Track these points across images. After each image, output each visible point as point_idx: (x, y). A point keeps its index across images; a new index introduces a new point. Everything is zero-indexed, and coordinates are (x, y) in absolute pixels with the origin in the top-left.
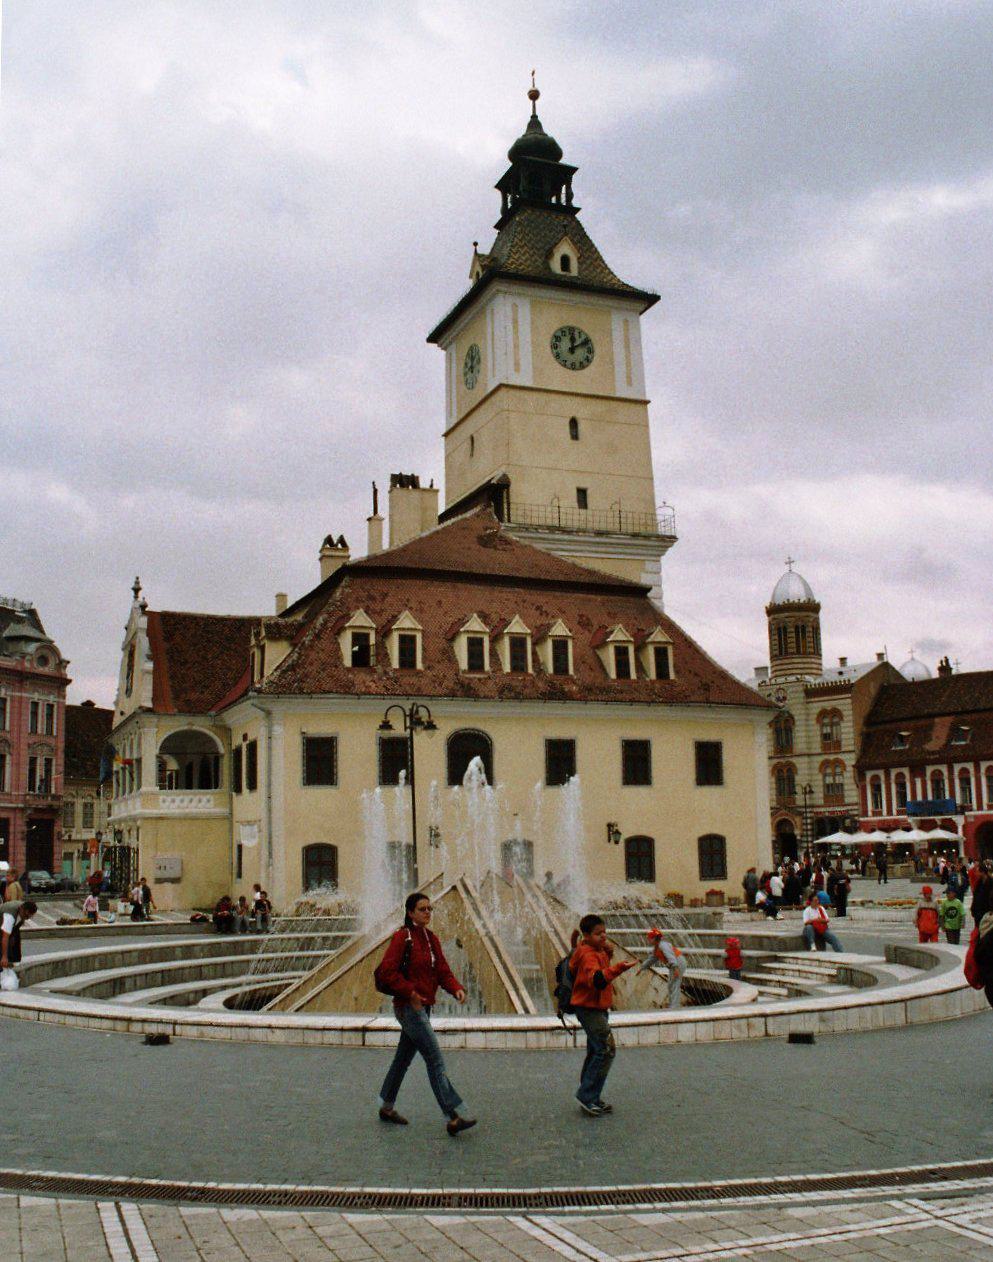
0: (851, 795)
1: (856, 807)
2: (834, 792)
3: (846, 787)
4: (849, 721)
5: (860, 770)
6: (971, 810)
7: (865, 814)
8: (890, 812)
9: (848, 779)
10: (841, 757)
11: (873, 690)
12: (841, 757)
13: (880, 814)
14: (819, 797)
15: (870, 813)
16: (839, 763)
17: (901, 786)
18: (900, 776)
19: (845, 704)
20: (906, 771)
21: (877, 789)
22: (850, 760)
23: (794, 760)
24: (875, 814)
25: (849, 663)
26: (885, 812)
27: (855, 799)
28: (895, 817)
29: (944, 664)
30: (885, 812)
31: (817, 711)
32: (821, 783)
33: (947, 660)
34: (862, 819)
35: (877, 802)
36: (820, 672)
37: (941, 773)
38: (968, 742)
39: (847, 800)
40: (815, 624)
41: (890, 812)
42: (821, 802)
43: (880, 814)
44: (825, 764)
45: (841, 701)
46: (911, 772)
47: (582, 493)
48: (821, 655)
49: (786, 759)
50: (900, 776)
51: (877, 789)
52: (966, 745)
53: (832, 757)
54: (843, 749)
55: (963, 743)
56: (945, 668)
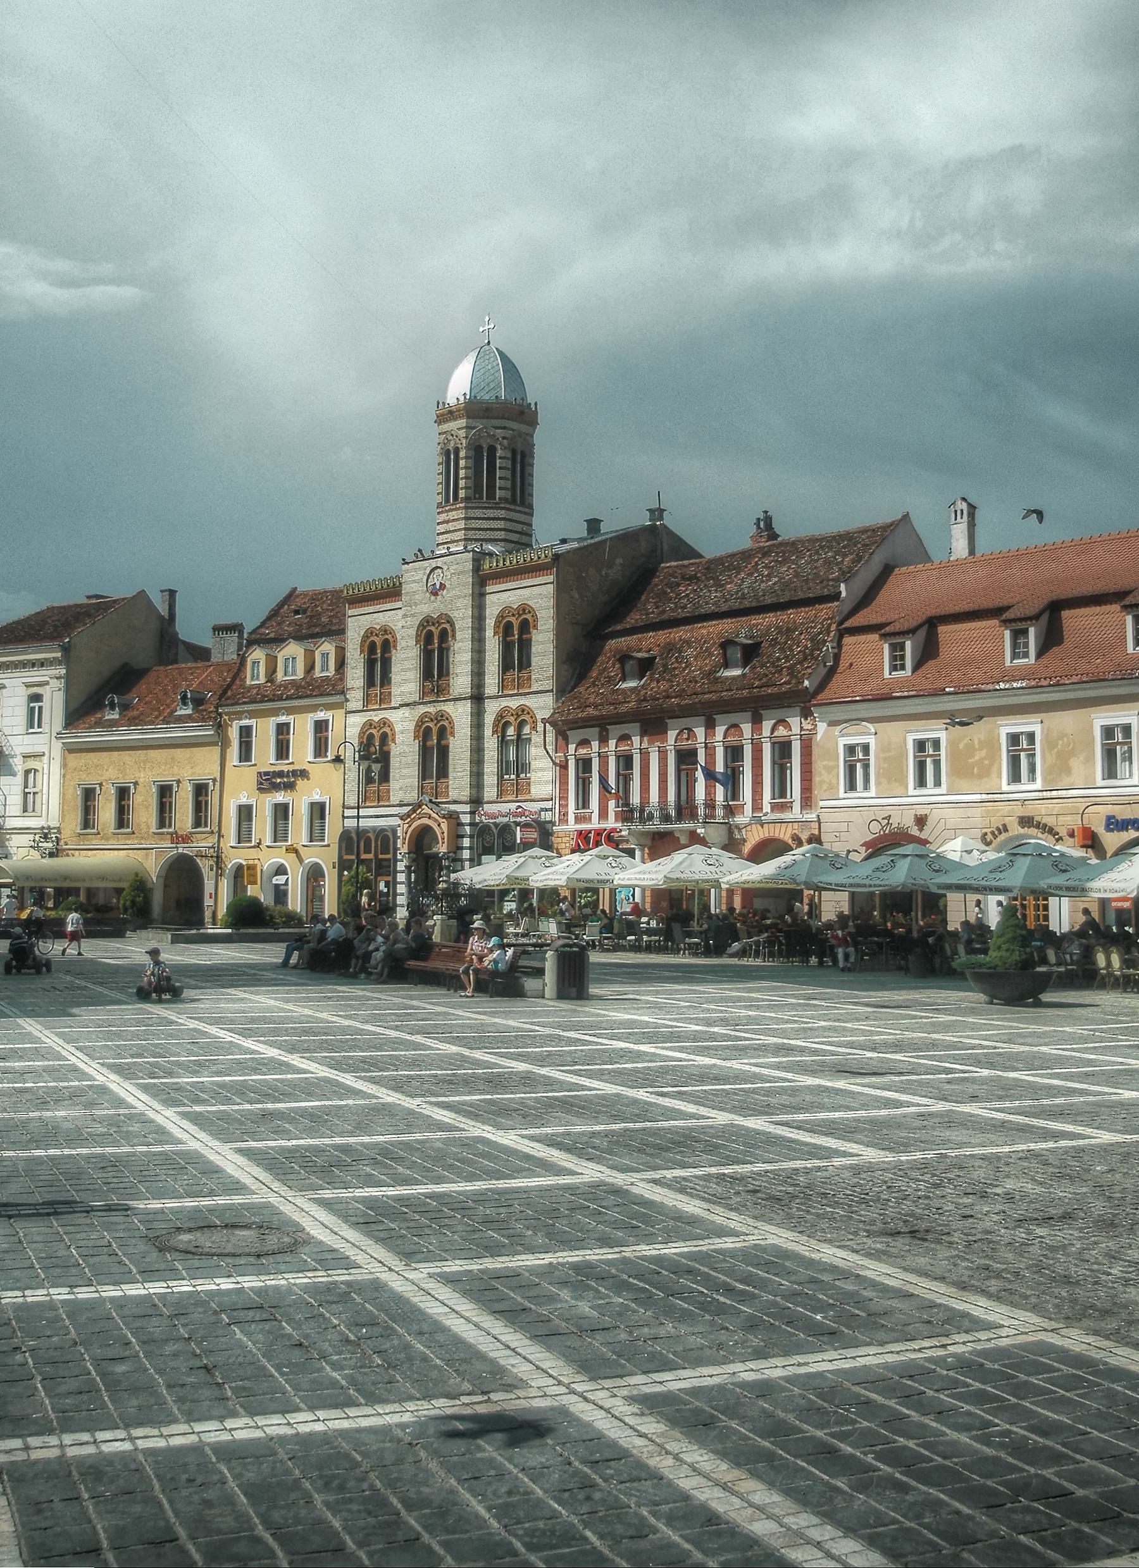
1: (549, 805)
8: (603, 814)
10: (530, 702)
12: (530, 702)
13: (588, 819)
15: (571, 817)
16: (523, 716)
23: (449, 708)
24: (579, 819)
25: (604, 528)
26: (595, 816)
28: (611, 823)
29: (762, 524)
33: (768, 520)
36: (524, 539)
39: (536, 791)
40: (519, 447)
43: (588, 819)
45: (536, 590)
48: (531, 507)
52: (744, 675)
53: (514, 703)
54: (534, 688)
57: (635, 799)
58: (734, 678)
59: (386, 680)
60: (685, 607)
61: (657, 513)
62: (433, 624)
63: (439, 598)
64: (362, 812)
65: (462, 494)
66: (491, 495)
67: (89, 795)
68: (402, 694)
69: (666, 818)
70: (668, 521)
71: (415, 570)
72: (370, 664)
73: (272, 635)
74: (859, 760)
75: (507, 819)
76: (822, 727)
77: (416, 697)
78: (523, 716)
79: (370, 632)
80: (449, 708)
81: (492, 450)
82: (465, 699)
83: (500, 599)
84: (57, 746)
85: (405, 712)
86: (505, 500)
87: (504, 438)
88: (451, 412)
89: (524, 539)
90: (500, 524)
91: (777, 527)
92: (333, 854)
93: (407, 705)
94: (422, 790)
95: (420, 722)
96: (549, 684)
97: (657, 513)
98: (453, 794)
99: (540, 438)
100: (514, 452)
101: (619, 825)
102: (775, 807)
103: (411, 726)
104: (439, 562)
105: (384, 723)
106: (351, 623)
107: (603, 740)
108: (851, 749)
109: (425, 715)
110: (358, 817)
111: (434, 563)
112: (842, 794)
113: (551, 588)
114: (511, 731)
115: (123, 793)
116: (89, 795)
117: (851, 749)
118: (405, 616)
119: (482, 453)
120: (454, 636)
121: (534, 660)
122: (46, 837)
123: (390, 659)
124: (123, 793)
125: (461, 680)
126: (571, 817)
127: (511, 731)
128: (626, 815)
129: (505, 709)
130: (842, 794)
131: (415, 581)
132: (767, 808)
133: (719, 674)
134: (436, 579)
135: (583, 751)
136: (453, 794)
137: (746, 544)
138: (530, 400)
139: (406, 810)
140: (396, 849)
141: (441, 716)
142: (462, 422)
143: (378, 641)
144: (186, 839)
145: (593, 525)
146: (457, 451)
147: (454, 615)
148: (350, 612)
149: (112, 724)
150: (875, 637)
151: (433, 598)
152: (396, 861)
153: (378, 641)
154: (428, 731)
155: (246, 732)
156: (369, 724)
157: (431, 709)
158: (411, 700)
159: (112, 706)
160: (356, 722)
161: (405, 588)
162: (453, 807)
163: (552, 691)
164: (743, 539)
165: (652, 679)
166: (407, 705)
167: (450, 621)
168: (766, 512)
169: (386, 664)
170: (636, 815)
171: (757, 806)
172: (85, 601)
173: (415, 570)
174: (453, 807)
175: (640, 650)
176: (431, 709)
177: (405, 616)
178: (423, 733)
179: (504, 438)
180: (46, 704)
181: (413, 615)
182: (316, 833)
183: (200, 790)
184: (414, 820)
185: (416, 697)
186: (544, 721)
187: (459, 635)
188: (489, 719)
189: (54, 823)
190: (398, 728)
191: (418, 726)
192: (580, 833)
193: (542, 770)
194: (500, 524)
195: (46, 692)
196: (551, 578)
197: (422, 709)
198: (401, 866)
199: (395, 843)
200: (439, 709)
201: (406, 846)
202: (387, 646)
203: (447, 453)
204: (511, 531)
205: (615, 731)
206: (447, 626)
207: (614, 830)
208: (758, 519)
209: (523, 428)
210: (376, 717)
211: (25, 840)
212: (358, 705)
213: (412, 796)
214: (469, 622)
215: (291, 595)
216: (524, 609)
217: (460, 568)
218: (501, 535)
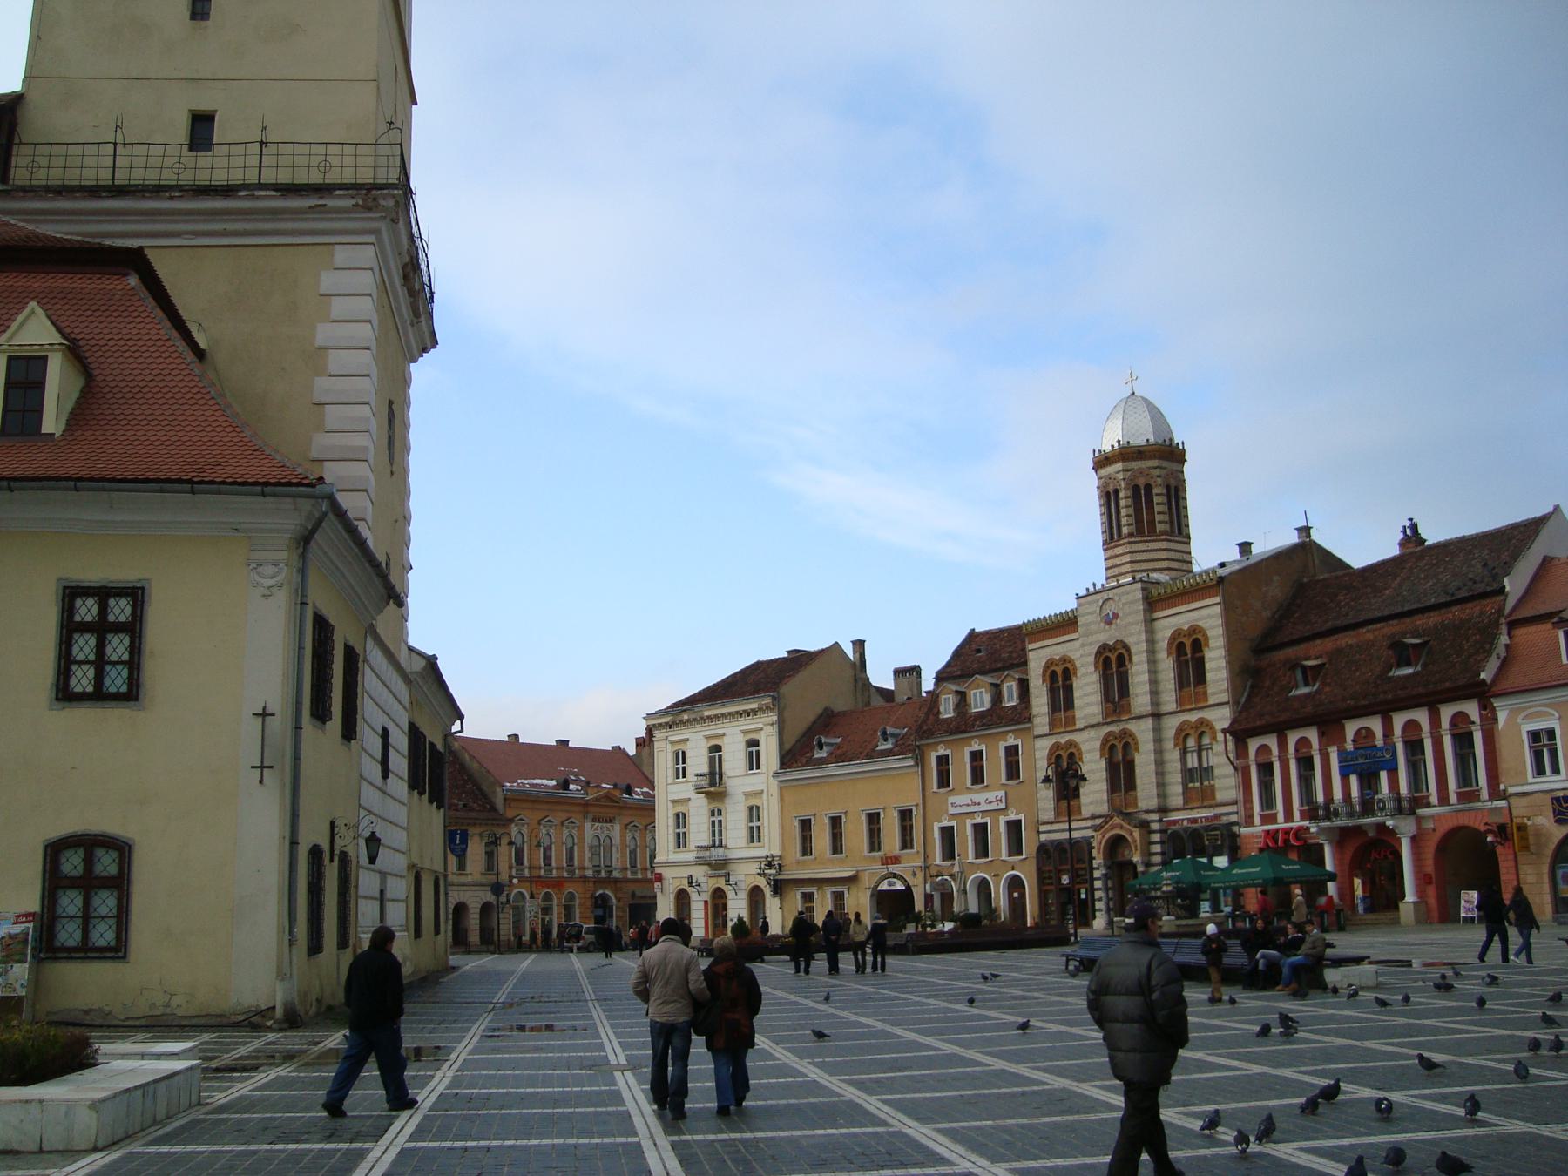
0: (1225, 784)
2: (1198, 780)
3: (1217, 772)
4: (1219, 648)
5: (1240, 734)
6: (1428, 805)
7: (1249, 821)
8: (1289, 816)
9: (1219, 757)
10: (1208, 715)
11: (1276, 590)
12: (1208, 715)
14: (1176, 796)
15: (1257, 820)
16: (1202, 728)
17: (1306, 763)
18: (1303, 743)
19: (1210, 617)
20: (1312, 735)
21: (1266, 769)
22: (1221, 718)
23: (1132, 726)
24: (1266, 819)
25: (1255, 550)
26: (1281, 817)
27: (1231, 794)
28: (1297, 822)
30: (1281, 817)
31: (1168, 633)
32: (1178, 766)
33: (1414, 527)
34: (1244, 831)
35: (1268, 801)
36: (1185, 567)
37: (1369, 733)
38: (1419, 668)
39: (1220, 796)
40: (1173, 483)
41: (1289, 816)
43: (1271, 819)
44: (1182, 734)
46: (1322, 734)
47: (201, 127)
48: (1188, 537)
49: (1122, 726)
50: (1303, 743)
51: (1266, 769)
52: (1415, 674)
53: (1193, 717)
54: (1211, 701)
55: (1408, 671)
56: (1412, 536)
57: (1320, 798)
58: (1407, 677)
59: (1069, 704)
60: (1347, 614)
61: (1305, 530)
62: (1110, 651)
63: (1113, 626)
64: (1074, 825)
65: (1125, 530)
66: (1152, 531)
67: (806, 825)
68: (1085, 717)
69: (1351, 815)
70: (1316, 536)
71: (1089, 603)
72: (1053, 692)
73: (959, 673)
74: (1545, 746)
76: (1502, 716)
77: (1099, 719)
78: (1202, 728)
79: (1050, 663)
80: (1132, 726)
81: (1148, 488)
82: (1146, 716)
83: (1172, 621)
84: (774, 784)
85: (1092, 733)
86: (1163, 533)
87: (1159, 476)
88: (1107, 458)
89: (1185, 567)
90: (1164, 555)
91: (1424, 532)
92: (1032, 867)
93: (1092, 726)
94: (1111, 802)
95: (1105, 741)
96: (1225, 697)
97: (1305, 530)
99: (1192, 472)
100: (1168, 488)
101: (1306, 823)
102: (1463, 797)
103: (1098, 745)
104: (1111, 594)
105: (1071, 744)
106: (1031, 655)
108: (1535, 736)
109: (1109, 734)
110: (1070, 830)
111: (1105, 596)
112: (1530, 779)
113: (1218, 609)
114: (1191, 742)
115: (836, 822)
116: (806, 825)
117: (1535, 736)
118: (1083, 645)
119: (1141, 494)
120: (1130, 660)
121: (1209, 676)
122: (770, 865)
123: (1071, 686)
124: (836, 822)
125: (1140, 699)
126: (1257, 820)
127: (1191, 742)
128: (1311, 813)
129: (1185, 722)
130: (1530, 779)
131: (1089, 613)
132: (1453, 798)
133: (1391, 674)
134: (1109, 610)
137: (1394, 551)
138: (1177, 440)
139: (1098, 821)
140: (1091, 858)
141: (1125, 733)
142: (1119, 466)
143: (1059, 670)
144: (896, 860)
145: (1245, 547)
146: (1116, 492)
147: (1129, 640)
148: (1030, 647)
149: (821, 762)
150: (1549, 626)
151: (1107, 627)
152: (1092, 869)
153: (1059, 670)
154: (1112, 747)
155: (942, 761)
156: (1057, 746)
157: (1115, 728)
158: (1094, 722)
159: (821, 746)
160: (1043, 748)
161: (1081, 621)
163: (1227, 703)
164: (1386, 547)
165: (1324, 684)
166: (1092, 726)
167: (1126, 647)
168: (1411, 520)
169: (1069, 690)
170: (1321, 812)
171: (1444, 799)
172: (786, 655)
173: (1089, 603)
175: (1307, 659)
176: (1115, 728)
177: (1083, 645)
178: (1108, 748)
179: (1159, 476)
180: (762, 748)
181: (1091, 644)
182: (1015, 847)
183: (906, 815)
184: (1107, 831)
185: (1099, 719)
186: (1224, 731)
187: (1135, 658)
188: (1445, 723)
189: (776, 852)
190: (1083, 748)
191: (1103, 745)
192: (1267, 832)
193: (1226, 776)
194: (1164, 555)
195: (762, 738)
196: (1217, 599)
197: (1106, 730)
198: (1097, 874)
199: (1090, 853)
201: (1101, 855)
202: (1068, 674)
203: (1108, 495)
204: (1173, 560)
206: (1124, 651)
207: (1299, 829)
208: (1405, 527)
209: (1175, 466)
210: (1063, 739)
211: (753, 868)
212: (1046, 730)
213: (1104, 809)
214: (1144, 646)
215: (972, 635)
216: (1195, 629)
217: (1130, 597)
218: (1165, 564)
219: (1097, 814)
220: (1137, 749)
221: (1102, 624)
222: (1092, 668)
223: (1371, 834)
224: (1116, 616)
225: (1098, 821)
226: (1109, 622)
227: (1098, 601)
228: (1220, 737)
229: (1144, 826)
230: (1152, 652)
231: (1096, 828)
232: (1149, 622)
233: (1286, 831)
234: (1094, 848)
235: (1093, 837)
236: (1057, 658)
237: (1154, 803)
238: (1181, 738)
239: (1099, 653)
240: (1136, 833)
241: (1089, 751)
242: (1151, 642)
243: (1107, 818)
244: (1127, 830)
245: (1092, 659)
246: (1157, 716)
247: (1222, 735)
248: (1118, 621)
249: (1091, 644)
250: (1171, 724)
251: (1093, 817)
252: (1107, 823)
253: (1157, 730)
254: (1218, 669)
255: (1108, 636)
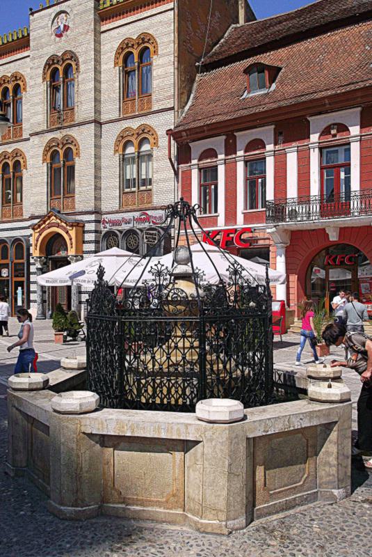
2: (136, 188)
8: (231, 215)
10: (150, 121)
14: (110, 200)
22: (163, 123)
28: (240, 223)
41: (231, 215)
42: (116, 206)
43: (214, 221)
44: (124, 141)
49: (65, 132)
53: (135, 124)
54: (155, 108)
63: (63, 38)
71: (41, 17)
75: (131, 225)
78: (144, 135)
80: (74, 132)
85: (35, 140)
93: (37, 134)
95: (48, 147)
98: (79, 207)
107: (230, 149)
109: (53, 140)
125: (84, 109)
129: (127, 129)
131: (41, 28)
135: (207, 162)
136: (79, 207)
139: (36, 221)
140: (29, 255)
147: (79, 51)
151: (58, 39)
152: (29, 264)
157: (58, 135)
162: (79, 218)
163: (173, 108)
166: (37, 134)
173: (41, 17)
174: (79, 218)
176: (58, 135)
184: (44, 229)
187: (82, 68)
191: (46, 151)
193: (165, 180)
196: (171, 5)
197: (50, 136)
199: (28, 250)
200: (65, 134)
205: (243, 138)
207: (245, 230)
213: (43, 210)
219: (36, 214)
220: (78, 154)
221: (53, 37)
222: (41, 80)
223: (333, 237)
224: (66, 28)
225: (36, 221)
226: (60, 36)
227: (50, 15)
228: (163, 141)
229: (79, 225)
230: (97, 61)
231: (33, 227)
232: (98, 33)
233: (227, 232)
234: (31, 245)
235: (31, 235)
236: (9, 75)
237: (91, 207)
238: (122, 144)
239: (48, 65)
240: (73, 233)
241: (32, 157)
242: (97, 52)
243: (44, 218)
244: (64, 229)
245: (41, 71)
246: (98, 123)
247: (167, 138)
248: (69, 32)
249: (40, 57)
250: (111, 134)
251: (32, 218)
252: (44, 222)
253: (98, 136)
254: (166, 75)
255: (57, 48)
